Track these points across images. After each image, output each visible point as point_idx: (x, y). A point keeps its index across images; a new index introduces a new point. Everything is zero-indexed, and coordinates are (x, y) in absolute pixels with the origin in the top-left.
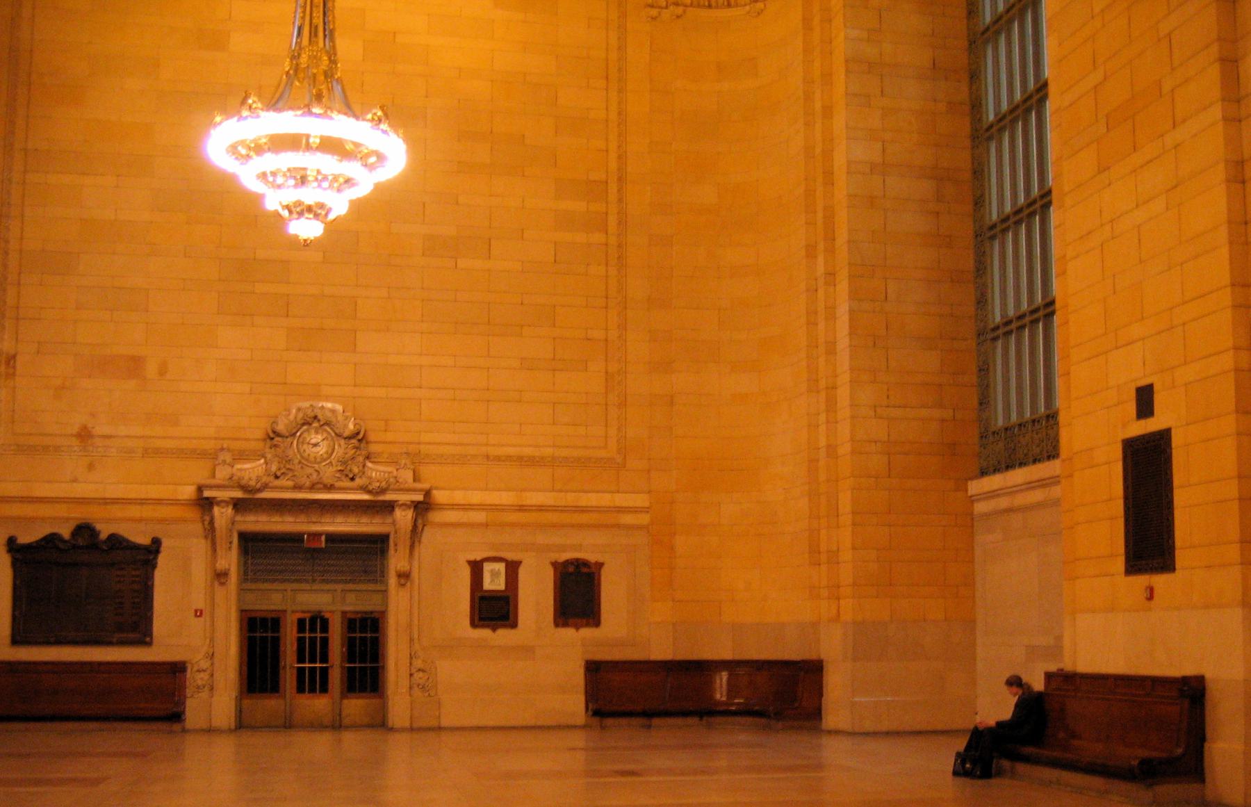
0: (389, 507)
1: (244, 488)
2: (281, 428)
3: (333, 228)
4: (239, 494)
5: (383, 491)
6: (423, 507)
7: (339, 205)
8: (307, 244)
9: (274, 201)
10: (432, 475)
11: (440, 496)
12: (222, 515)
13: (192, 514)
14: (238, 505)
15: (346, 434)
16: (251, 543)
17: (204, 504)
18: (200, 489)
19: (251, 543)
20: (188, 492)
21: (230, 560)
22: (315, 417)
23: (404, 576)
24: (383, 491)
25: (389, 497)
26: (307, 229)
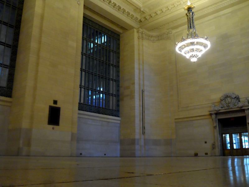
0: (244, 110)
3: (199, 59)
4: (215, 112)
7: (200, 55)
8: (194, 62)
9: (188, 56)
13: (209, 117)
15: (234, 97)
16: (220, 121)
17: (211, 115)
20: (208, 113)
21: (216, 124)
22: (227, 96)
24: (242, 107)
25: (243, 108)
26: (194, 60)
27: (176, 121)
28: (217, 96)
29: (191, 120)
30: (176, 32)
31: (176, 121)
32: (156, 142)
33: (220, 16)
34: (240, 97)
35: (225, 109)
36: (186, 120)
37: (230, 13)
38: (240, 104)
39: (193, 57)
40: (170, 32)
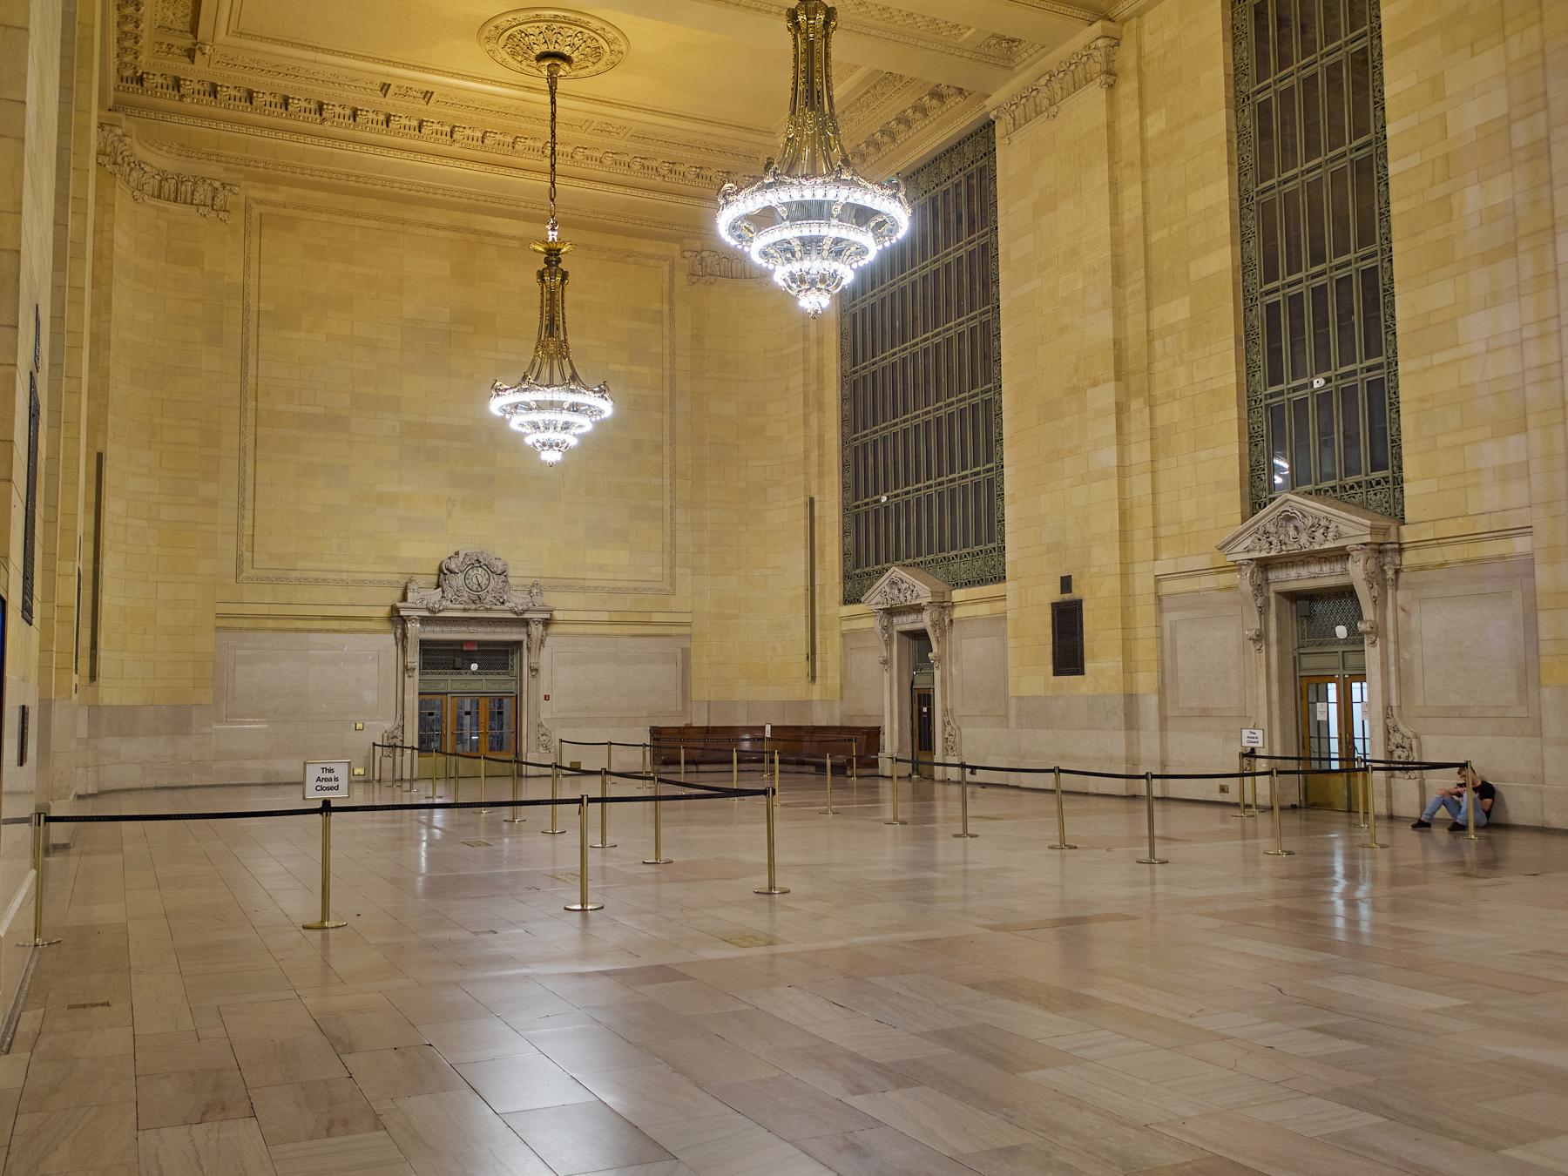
0: (526, 623)
1: (429, 609)
2: (453, 566)
4: (426, 614)
5: (524, 611)
6: (547, 623)
10: (550, 599)
11: (558, 615)
12: (414, 628)
13: (386, 626)
14: (424, 621)
16: (426, 647)
17: (397, 619)
18: (394, 609)
19: (426, 647)
20: (384, 612)
21: (414, 659)
23: (535, 670)
24: (524, 611)
25: (526, 616)
27: (223, 623)
28: (426, 552)
29: (298, 630)
30: (261, 202)
31: (223, 623)
32: (122, 721)
33: (474, 232)
34: (510, 572)
35: (465, 610)
36: (270, 623)
37: (514, 238)
38: (517, 600)
39: (551, 446)
40: (236, 190)
